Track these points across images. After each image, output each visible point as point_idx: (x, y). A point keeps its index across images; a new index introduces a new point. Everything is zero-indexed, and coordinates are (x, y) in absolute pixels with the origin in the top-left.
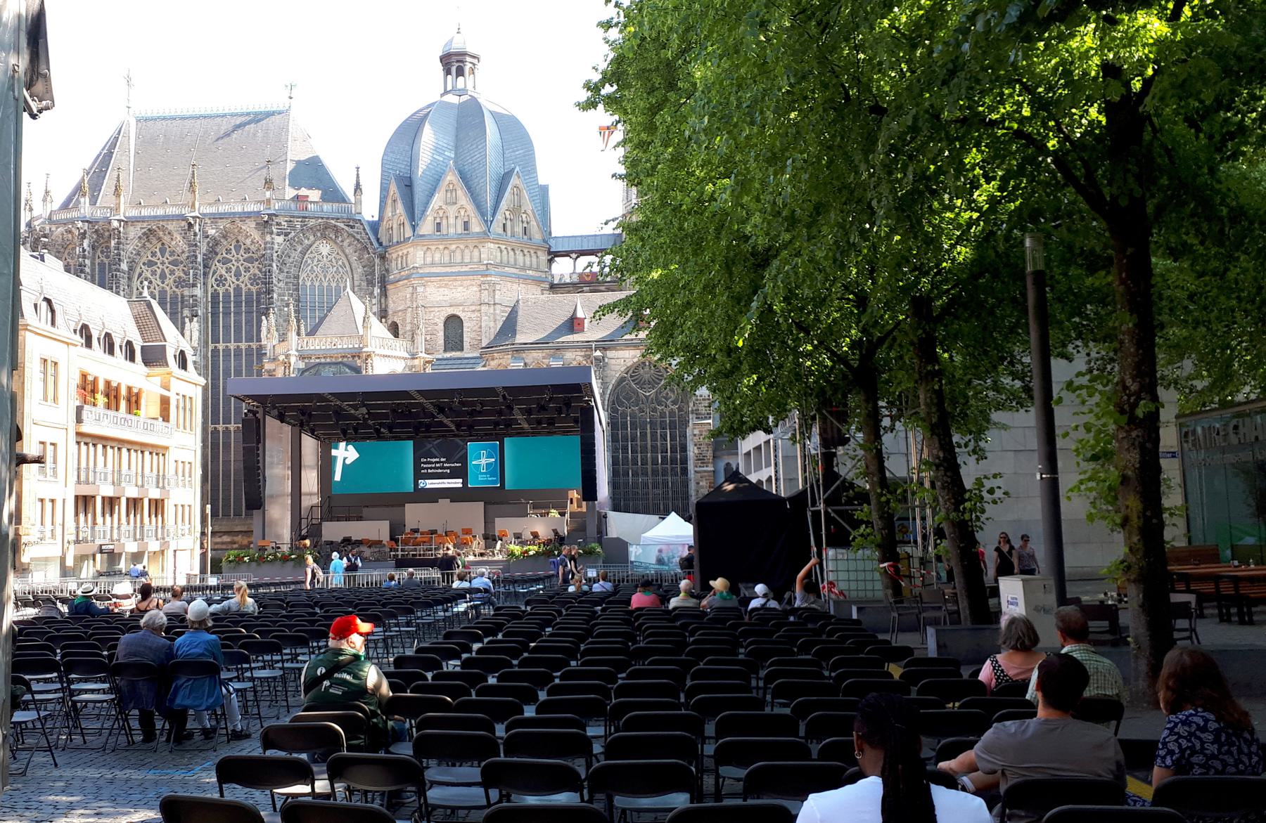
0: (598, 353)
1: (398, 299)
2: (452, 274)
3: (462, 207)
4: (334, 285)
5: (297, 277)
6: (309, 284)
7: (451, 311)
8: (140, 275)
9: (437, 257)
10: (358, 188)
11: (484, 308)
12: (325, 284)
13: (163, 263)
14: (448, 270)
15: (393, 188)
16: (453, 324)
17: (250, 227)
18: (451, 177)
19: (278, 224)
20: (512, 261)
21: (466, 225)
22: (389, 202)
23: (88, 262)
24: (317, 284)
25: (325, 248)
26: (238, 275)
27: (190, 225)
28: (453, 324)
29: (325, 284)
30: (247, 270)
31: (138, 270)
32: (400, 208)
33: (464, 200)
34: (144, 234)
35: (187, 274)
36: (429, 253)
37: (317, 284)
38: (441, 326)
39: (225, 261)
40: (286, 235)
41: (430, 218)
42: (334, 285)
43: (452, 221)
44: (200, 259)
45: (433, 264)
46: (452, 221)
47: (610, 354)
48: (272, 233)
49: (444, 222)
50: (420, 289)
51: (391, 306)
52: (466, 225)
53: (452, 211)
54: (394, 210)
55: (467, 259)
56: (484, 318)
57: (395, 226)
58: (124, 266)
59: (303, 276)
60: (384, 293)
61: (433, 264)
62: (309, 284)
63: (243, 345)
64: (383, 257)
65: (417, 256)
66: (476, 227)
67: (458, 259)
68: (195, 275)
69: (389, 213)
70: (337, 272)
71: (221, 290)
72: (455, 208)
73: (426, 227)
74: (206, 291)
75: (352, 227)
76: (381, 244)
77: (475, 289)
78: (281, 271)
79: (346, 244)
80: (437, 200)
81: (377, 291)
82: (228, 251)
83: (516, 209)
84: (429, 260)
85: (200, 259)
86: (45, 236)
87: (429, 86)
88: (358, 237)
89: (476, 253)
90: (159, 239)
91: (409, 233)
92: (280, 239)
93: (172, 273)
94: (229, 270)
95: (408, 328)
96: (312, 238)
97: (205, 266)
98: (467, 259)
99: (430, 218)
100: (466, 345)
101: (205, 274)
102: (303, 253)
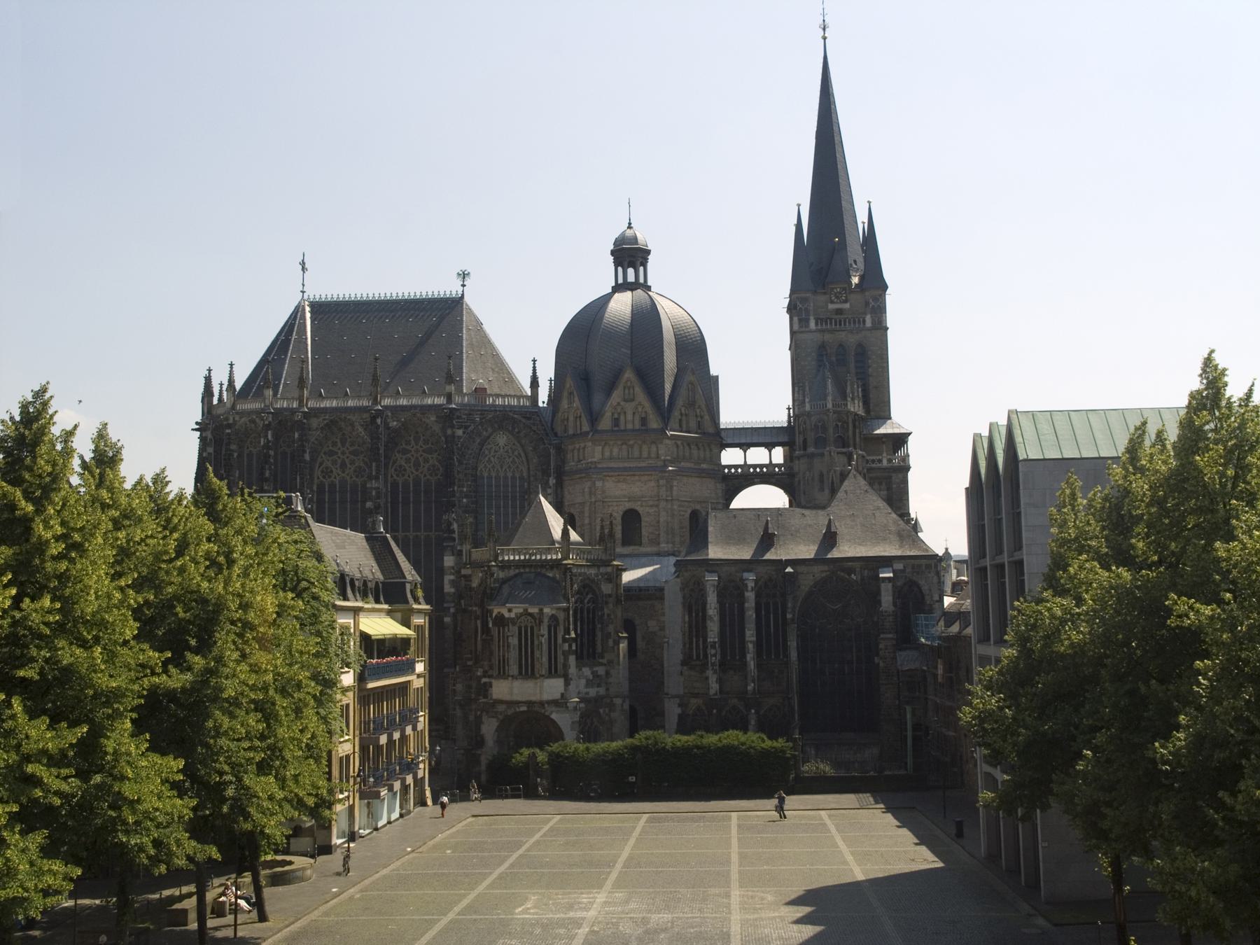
0: (789, 570)
1: (575, 493)
2: (625, 469)
3: (640, 404)
4: (510, 475)
5: (476, 468)
6: (486, 475)
7: (628, 506)
8: (321, 464)
9: (615, 451)
10: (535, 383)
11: (663, 504)
12: (502, 474)
13: (343, 453)
14: (626, 465)
15: (569, 383)
16: (631, 518)
17: (433, 418)
18: (629, 375)
19: (459, 417)
20: (687, 454)
21: (644, 421)
22: (565, 394)
23: (272, 453)
24: (494, 474)
25: (502, 439)
26: (417, 465)
27: (374, 418)
28: (631, 518)
29: (502, 474)
30: (426, 461)
31: (319, 460)
32: (577, 403)
33: (641, 396)
34: (327, 425)
35: (370, 467)
36: (607, 449)
37: (494, 474)
38: (619, 519)
39: (405, 452)
40: (466, 428)
41: (608, 414)
42: (510, 475)
43: (630, 417)
44: (382, 451)
45: (611, 458)
46: (630, 417)
47: (801, 569)
48: (452, 427)
49: (622, 418)
50: (599, 484)
51: (567, 497)
52: (644, 421)
53: (629, 407)
54: (570, 403)
55: (645, 454)
56: (663, 514)
57: (571, 418)
58: (307, 457)
59: (481, 467)
60: (560, 484)
61: (611, 458)
62: (486, 475)
63: (422, 534)
64: (559, 449)
65: (595, 453)
66: (654, 424)
67: (636, 454)
68: (378, 466)
69: (564, 404)
70: (513, 462)
71: (400, 481)
72: (633, 404)
73: (605, 423)
74: (386, 482)
75: (529, 419)
76: (556, 435)
77: (653, 484)
78: (460, 463)
79: (522, 434)
80: (616, 396)
81: (552, 481)
82: (408, 443)
83: (692, 404)
84: (607, 454)
85: (382, 451)
86: (229, 426)
87: (599, 276)
88: (534, 428)
89: (654, 449)
90: (340, 429)
91: (586, 428)
92: (460, 432)
93: (352, 463)
94: (408, 461)
95: (587, 521)
96: (490, 430)
97: (386, 457)
98: (645, 454)
99: (608, 414)
100: (645, 540)
101: (386, 465)
102: (482, 445)
